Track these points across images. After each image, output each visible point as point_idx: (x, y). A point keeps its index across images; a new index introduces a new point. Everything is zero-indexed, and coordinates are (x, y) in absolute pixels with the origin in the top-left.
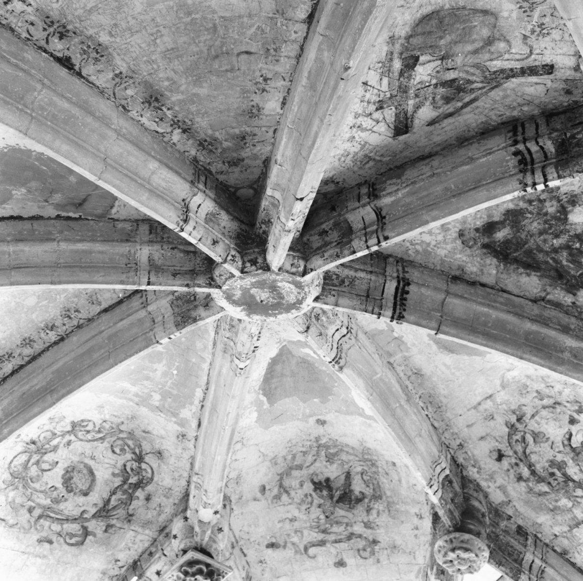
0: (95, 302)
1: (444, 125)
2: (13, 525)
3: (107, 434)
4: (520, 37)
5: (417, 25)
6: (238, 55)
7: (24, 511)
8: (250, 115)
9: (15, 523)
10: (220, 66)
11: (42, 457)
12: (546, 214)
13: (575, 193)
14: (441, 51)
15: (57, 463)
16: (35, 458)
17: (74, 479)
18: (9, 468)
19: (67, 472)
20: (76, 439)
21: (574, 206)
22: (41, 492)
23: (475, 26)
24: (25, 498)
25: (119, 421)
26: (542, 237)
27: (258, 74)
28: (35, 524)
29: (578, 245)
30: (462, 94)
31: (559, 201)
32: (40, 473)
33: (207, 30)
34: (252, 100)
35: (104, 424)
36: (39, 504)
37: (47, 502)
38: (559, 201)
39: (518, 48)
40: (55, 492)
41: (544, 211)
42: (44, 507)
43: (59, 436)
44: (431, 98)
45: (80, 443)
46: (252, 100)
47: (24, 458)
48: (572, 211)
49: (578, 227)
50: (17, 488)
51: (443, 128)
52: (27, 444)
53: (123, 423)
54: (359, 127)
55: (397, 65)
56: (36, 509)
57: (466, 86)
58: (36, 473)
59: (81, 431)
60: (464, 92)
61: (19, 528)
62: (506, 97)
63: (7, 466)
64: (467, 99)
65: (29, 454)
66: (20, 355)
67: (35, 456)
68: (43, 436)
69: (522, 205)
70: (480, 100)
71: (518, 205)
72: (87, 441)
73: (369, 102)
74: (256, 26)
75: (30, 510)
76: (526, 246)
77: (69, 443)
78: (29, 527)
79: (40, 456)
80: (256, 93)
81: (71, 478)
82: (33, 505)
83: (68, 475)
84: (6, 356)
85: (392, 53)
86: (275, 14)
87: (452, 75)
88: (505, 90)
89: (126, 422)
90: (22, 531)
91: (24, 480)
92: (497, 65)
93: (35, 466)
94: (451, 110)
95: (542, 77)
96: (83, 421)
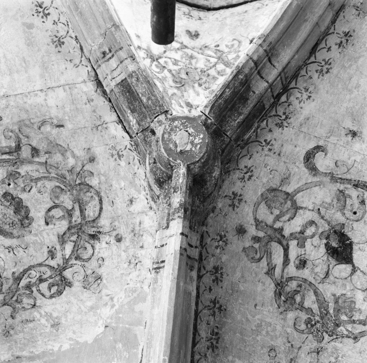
2: (42, 125)
3: (18, 289)
7: (42, 147)
9: (42, 128)
11: (70, 222)
15: (47, 224)
16: (77, 217)
17: (12, 212)
18: (98, 193)
19: (27, 217)
20: (47, 263)
22: (38, 179)
24: (52, 163)
25: (18, 318)
28: (18, 137)
32: (56, 201)
35: (31, 301)
36: (30, 162)
37: (23, 170)
40: (22, 185)
42: (22, 162)
43: (70, 258)
45: (40, 260)
47: (91, 212)
50: (71, 171)
52: (100, 232)
53: (13, 317)
56: (30, 156)
58: (61, 199)
59: (50, 277)
61: (33, 124)
63: (102, 194)
65: (88, 219)
66: (206, 355)
67: (79, 221)
68: (90, 251)
72: (33, 267)
75: (35, 151)
77: (52, 254)
78: (22, 130)
79: (74, 223)
81: (17, 211)
82: (37, 159)
83: (23, 213)
84: (214, 343)
89: (10, 320)
90: (27, 122)
91: (70, 186)
93: (70, 208)
96: (60, 293)
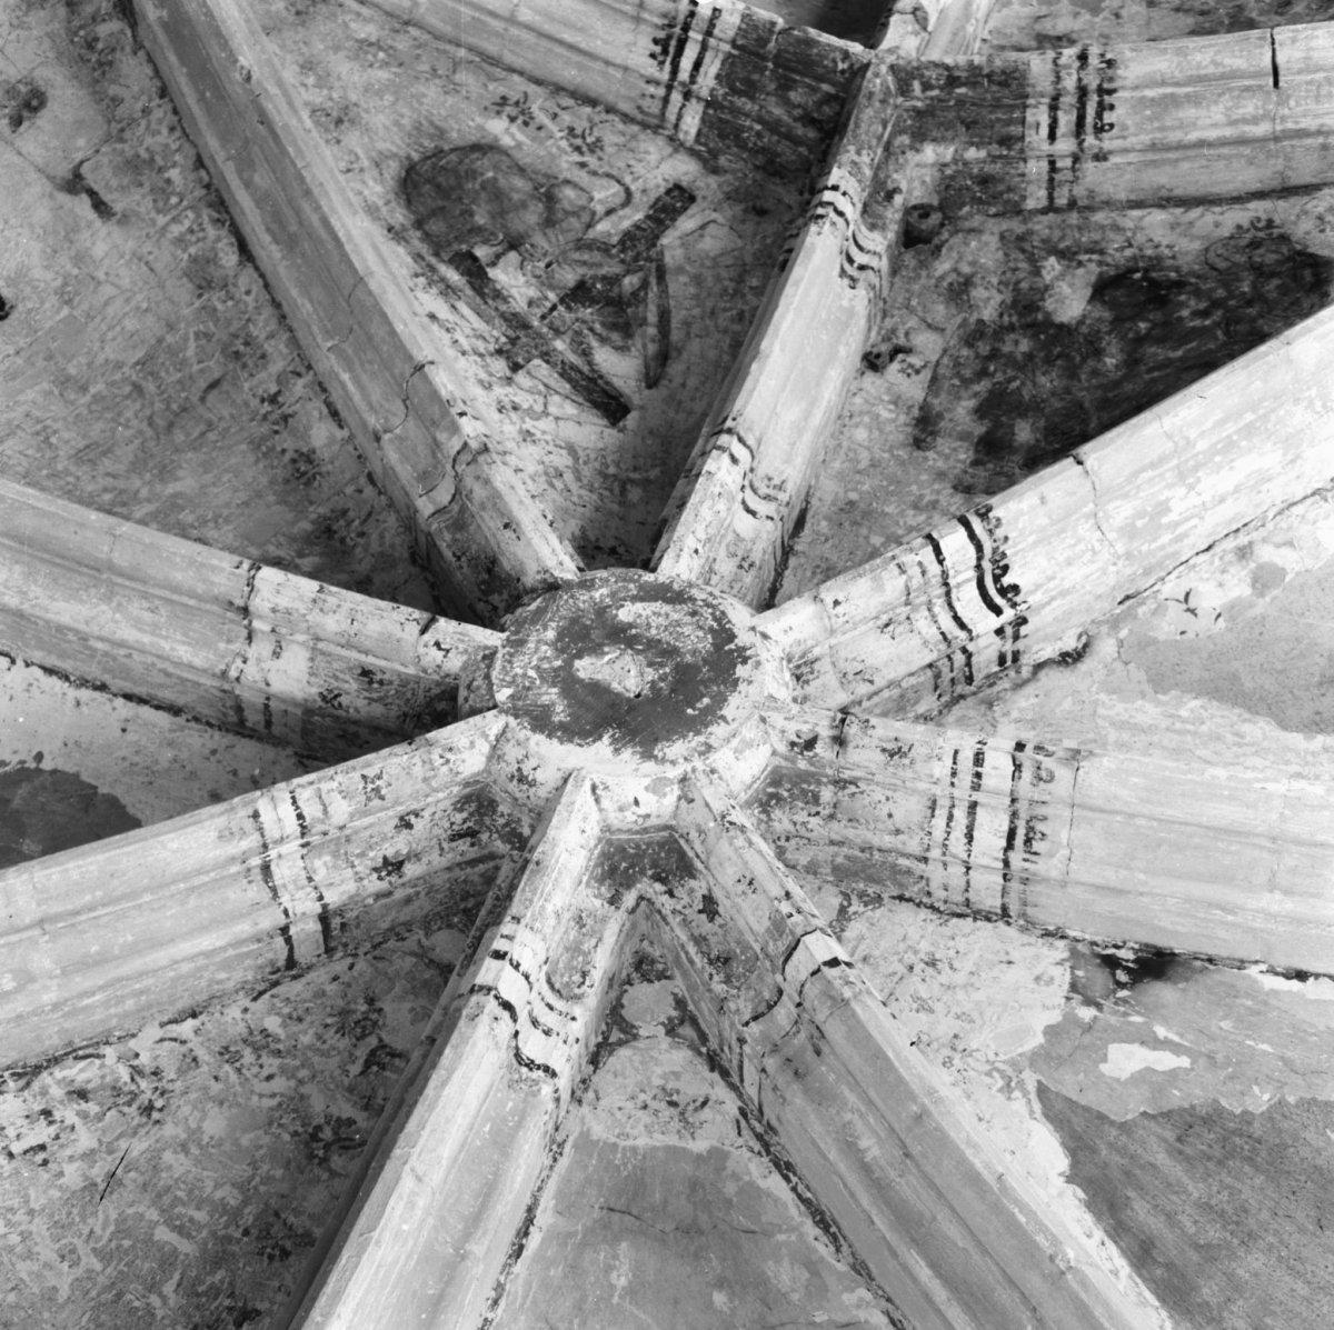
0: (288, 1245)
1: (678, 380)
6: (203, 399)
8: (303, 480)
10: (188, 435)
12: (1029, 356)
13: (1008, 301)
21: (1038, 309)
23: (495, 179)
26: (1083, 377)
27: (255, 403)
29: (1142, 325)
31: (1011, 328)
33: (127, 397)
34: (284, 451)
38: (1011, 328)
41: (1019, 357)
46: (284, 451)
48: (1048, 315)
49: (1096, 314)
51: (683, 385)
55: (453, 276)
62: (698, 280)
64: (652, 317)
69: (983, 387)
71: (976, 395)
74: (192, 336)
76: (1087, 405)
80: (276, 432)
86: (200, 296)
87: (569, 277)
88: (680, 270)
94: (652, 348)
95: (690, 212)
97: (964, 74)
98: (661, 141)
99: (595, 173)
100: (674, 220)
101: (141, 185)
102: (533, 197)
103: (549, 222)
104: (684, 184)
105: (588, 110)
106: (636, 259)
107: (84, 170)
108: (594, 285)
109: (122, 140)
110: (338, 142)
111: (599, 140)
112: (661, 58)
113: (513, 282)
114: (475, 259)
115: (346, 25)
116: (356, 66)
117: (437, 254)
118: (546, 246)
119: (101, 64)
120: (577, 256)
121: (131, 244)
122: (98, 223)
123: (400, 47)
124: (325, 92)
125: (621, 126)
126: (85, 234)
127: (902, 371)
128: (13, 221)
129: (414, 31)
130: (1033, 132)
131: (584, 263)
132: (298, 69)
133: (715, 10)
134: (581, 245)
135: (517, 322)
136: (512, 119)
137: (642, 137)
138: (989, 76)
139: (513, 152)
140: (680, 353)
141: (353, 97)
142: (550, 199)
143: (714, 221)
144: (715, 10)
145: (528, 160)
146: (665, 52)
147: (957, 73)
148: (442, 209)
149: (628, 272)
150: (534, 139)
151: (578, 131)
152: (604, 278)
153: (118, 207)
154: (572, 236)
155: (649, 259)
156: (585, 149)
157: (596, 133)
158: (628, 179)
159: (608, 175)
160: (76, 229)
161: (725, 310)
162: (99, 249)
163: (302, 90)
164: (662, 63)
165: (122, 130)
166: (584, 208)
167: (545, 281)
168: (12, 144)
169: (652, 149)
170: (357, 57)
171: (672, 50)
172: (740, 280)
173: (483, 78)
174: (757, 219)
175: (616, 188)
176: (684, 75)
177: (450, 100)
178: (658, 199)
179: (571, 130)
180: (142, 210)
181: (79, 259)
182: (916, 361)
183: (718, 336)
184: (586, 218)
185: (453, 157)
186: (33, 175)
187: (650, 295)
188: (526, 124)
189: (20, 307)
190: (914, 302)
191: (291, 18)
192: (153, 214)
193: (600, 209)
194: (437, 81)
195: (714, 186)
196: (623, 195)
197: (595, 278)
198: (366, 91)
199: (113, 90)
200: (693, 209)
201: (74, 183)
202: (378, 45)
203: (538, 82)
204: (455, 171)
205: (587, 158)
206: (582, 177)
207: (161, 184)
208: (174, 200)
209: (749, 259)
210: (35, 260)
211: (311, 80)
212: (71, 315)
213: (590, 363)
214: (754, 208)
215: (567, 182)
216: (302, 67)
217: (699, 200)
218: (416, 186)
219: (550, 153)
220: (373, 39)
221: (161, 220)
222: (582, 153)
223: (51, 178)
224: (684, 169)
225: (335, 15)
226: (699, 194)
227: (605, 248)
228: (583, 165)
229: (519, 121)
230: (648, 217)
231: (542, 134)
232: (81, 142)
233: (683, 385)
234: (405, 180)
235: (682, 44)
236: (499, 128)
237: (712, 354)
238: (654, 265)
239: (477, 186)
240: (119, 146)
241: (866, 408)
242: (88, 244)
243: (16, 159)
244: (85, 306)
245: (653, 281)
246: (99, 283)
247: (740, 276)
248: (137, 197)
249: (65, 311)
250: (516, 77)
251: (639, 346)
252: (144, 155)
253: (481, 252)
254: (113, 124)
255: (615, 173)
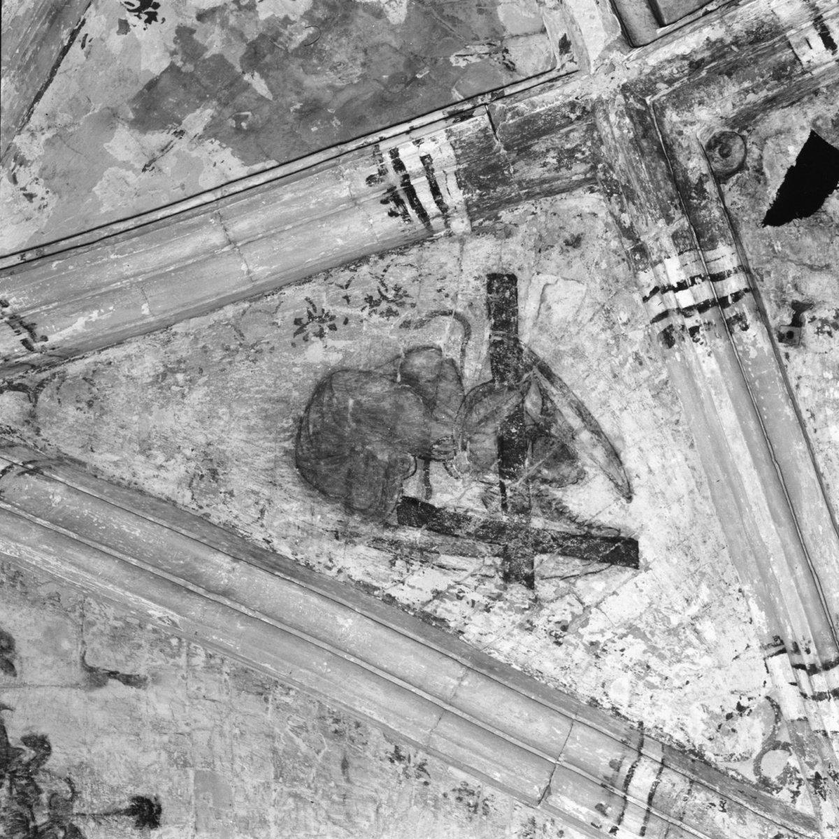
1: (643, 470)
4: (403, 332)
5: (323, 492)
6: (348, 780)
8: (480, 811)
10: (368, 818)
14: (404, 461)
23: (358, 403)
27: (387, 765)
30: (553, 431)
33: (297, 809)
34: (445, 795)
39: (444, 336)
44: (542, 487)
46: (445, 795)
54: (564, 628)
55: (414, 535)
57: (528, 421)
60: (549, 426)
64: (576, 422)
70: (583, 399)
73: (499, 597)
74: (292, 734)
80: (426, 783)
85: (378, 540)
86: (266, 700)
87: (487, 444)
92: (475, 368)
94: (599, 453)
95: (521, 293)
97: (707, 54)
98: (444, 245)
99: (421, 324)
100: (515, 313)
101: (140, 646)
102: (399, 392)
103: (430, 405)
104: (495, 269)
105: (365, 269)
106: (518, 377)
107: (90, 662)
108: (509, 432)
109: (91, 624)
110: (231, 494)
111: (397, 289)
112: (400, 210)
113: (457, 494)
114: (414, 501)
115: (131, 378)
116: (172, 408)
117: (387, 526)
118: (447, 432)
119: (13, 579)
120: (475, 418)
121: (180, 693)
122: (141, 692)
123: (184, 354)
124: (179, 457)
125: (402, 260)
126: (143, 707)
127: (819, 331)
128: (88, 740)
129: (179, 328)
130: (806, 48)
131: (486, 419)
132: (142, 458)
133: (423, 159)
134: (469, 403)
135: (492, 532)
136: (321, 335)
137: (426, 254)
138: (736, 42)
139: (348, 364)
140: (622, 439)
141: (201, 439)
142: (411, 380)
143: (547, 285)
144: (423, 159)
145: (364, 361)
146: (399, 202)
147: (699, 57)
148: (350, 474)
149: (523, 394)
150: (351, 337)
151: (376, 297)
152: (511, 418)
153: (142, 672)
154: (456, 403)
155: (528, 368)
156: (395, 308)
157: (391, 286)
158: (448, 305)
159: (433, 315)
160: (133, 709)
161: (622, 365)
162: (163, 710)
163: (163, 474)
164: (405, 213)
165: (82, 616)
166: (441, 364)
167: (478, 468)
168: (25, 685)
169: (443, 260)
170: (168, 400)
171: (403, 197)
172: (611, 325)
173: (267, 318)
174: (577, 252)
175: (448, 322)
176: (431, 207)
177: (263, 365)
178: (488, 304)
179: (369, 299)
180: (160, 662)
181: (158, 727)
182: (822, 313)
183: (636, 396)
184: (451, 374)
185: (314, 416)
186: (64, 695)
187: (555, 399)
188: (333, 328)
189: (162, 795)
190: (778, 247)
191: (91, 414)
192: (172, 661)
193: (454, 354)
194: (238, 358)
195: (519, 249)
196: (458, 324)
197: (504, 426)
198: (202, 422)
199: (43, 592)
200: (522, 287)
201: (96, 677)
202: (169, 371)
203: (308, 279)
204: (326, 427)
205: (405, 314)
206: (415, 337)
207: (153, 636)
208: (174, 642)
209: (601, 297)
210: (132, 752)
211: (160, 459)
212: (197, 772)
213: (572, 520)
214: (567, 243)
215: (409, 352)
216: (142, 452)
217: (518, 273)
218: (315, 473)
219: (373, 337)
220: (162, 369)
221: (182, 661)
222: (396, 314)
223: (76, 686)
224: (484, 253)
225: (115, 378)
226: (513, 269)
227: (487, 390)
228: (406, 325)
229: (327, 330)
230: (494, 327)
231: (353, 325)
232: (66, 645)
233: (650, 471)
234: (303, 475)
235: (411, 192)
236: (320, 354)
237: (646, 417)
238: (535, 370)
239: (354, 425)
240: (94, 629)
241: (818, 397)
242: (152, 712)
243: (39, 693)
244: (199, 759)
245: (546, 384)
246: (189, 734)
247: (608, 319)
248: (147, 656)
249: (191, 773)
250: (288, 292)
251: (589, 462)
252: (119, 624)
253: (412, 489)
254: (72, 615)
255: (434, 308)
